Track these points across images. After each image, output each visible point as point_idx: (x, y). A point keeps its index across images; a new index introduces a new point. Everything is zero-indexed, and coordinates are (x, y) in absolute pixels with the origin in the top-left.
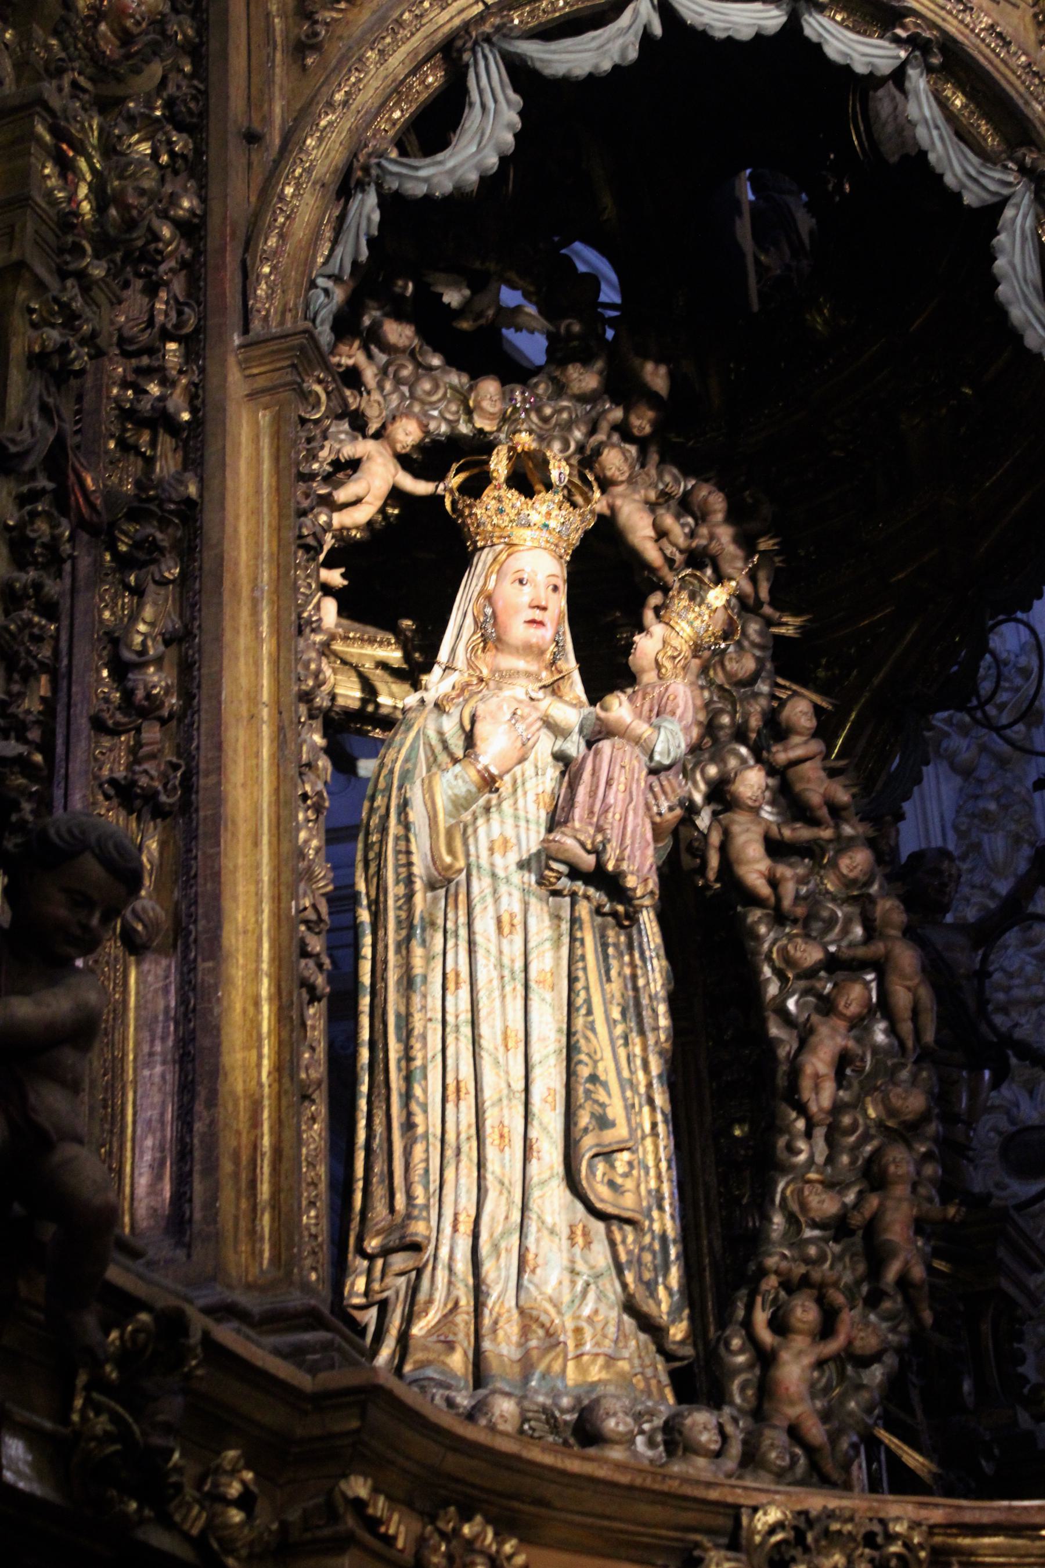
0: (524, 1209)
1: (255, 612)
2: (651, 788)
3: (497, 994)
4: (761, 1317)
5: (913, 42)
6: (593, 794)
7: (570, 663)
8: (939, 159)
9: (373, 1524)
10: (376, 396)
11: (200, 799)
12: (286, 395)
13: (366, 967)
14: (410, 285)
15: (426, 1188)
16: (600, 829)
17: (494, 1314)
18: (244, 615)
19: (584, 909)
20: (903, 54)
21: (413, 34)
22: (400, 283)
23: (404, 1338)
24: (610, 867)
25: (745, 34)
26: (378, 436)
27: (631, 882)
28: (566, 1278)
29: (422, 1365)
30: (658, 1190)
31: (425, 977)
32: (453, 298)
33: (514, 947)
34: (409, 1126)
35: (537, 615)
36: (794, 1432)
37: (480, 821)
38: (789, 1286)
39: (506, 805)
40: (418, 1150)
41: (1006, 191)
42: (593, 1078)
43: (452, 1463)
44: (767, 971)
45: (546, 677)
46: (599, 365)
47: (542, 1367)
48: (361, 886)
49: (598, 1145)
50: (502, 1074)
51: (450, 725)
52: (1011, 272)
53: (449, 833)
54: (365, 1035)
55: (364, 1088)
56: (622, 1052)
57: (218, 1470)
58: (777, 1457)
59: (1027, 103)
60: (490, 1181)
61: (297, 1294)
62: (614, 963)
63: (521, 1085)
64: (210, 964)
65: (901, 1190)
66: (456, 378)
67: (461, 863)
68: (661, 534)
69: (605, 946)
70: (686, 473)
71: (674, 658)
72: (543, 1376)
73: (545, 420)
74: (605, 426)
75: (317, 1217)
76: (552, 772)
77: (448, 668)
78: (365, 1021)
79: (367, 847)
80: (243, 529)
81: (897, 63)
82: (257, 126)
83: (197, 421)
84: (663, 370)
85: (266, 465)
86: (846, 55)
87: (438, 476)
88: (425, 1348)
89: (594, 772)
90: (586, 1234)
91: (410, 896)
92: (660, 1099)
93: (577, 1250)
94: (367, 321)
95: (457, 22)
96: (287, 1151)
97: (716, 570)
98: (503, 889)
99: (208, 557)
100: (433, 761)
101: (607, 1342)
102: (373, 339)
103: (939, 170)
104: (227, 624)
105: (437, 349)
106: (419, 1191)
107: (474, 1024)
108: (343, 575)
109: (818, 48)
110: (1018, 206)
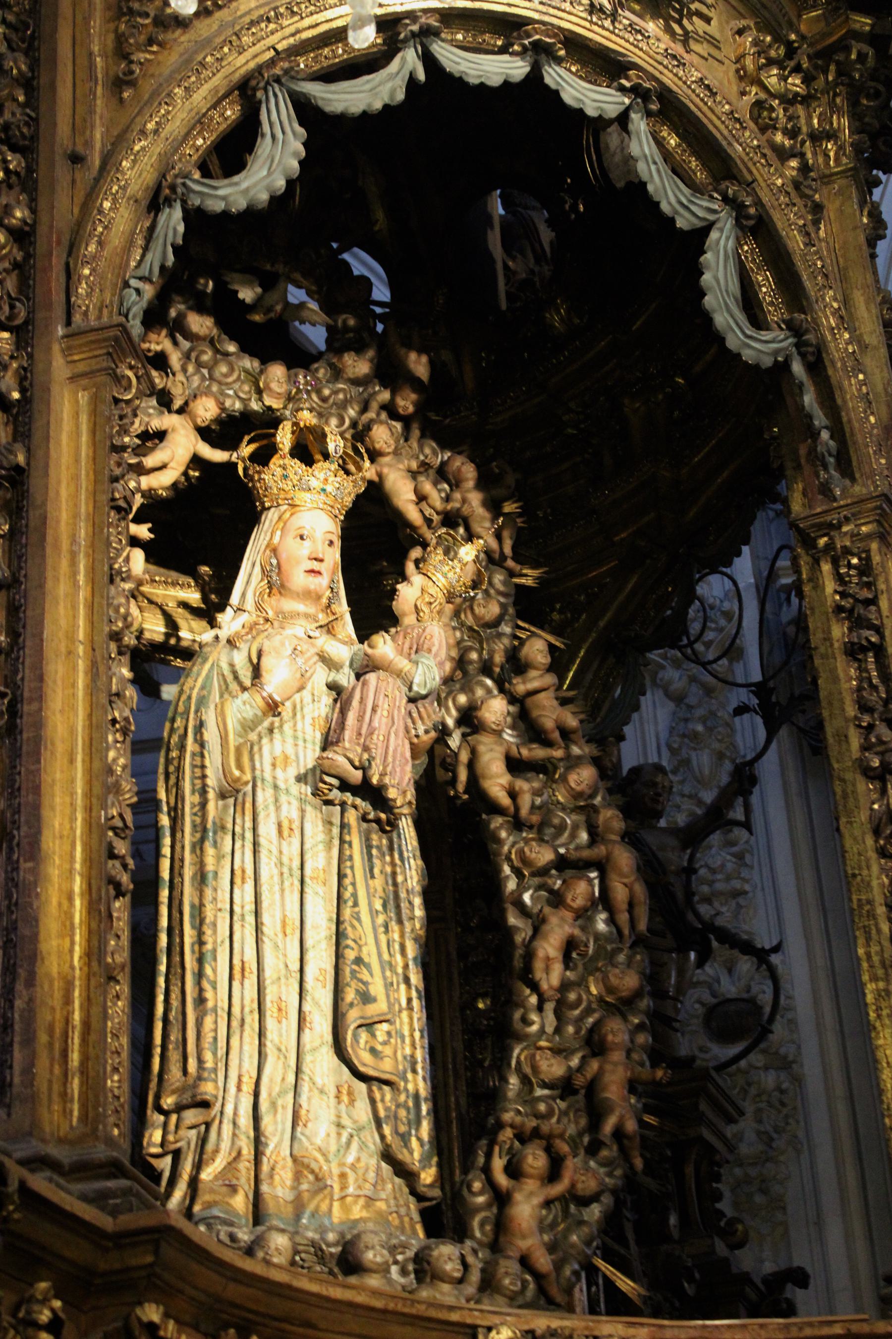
0: (298, 1071)
1: (73, 563)
2: (410, 713)
3: (277, 888)
4: (498, 1164)
5: (635, 90)
6: (360, 718)
7: (343, 608)
8: (656, 190)
10: (180, 377)
11: (24, 722)
12: (102, 378)
13: (165, 865)
14: (211, 283)
15: (215, 1054)
16: (366, 749)
17: (272, 1161)
18: (64, 564)
19: (352, 816)
20: (627, 101)
21: (214, 74)
22: (202, 281)
23: (194, 1183)
24: (375, 781)
25: (495, 81)
26: (181, 411)
27: (392, 793)
28: (333, 1130)
29: (209, 1205)
30: (412, 1056)
31: (216, 873)
32: (247, 294)
33: (292, 848)
34: (201, 1000)
35: (315, 565)
36: (525, 1262)
37: (265, 741)
38: (522, 1137)
39: (287, 727)
40: (208, 1021)
41: (711, 217)
42: (358, 961)
43: (234, 1291)
44: (507, 870)
45: (323, 619)
46: (371, 353)
47: (311, 1207)
48: (162, 795)
49: (362, 1018)
50: (281, 956)
51: (240, 659)
52: (715, 284)
53: (238, 750)
54: (164, 922)
55: (163, 968)
56: (383, 938)
57: (31, 1299)
58: (511, 1284)
59: (730, 144)
60: (270, 1049)
61: (101, 1147)
62: (377, 862)
63: (296, 966)
64: (30, 865)
65: (617, 1056)
66: (249, 363)
67: (248, 777)
68: (421, 498)
69: (369, 847)
70: (443, 446)
71: (431, 603)
72: (313, 1215)
73: (324, 400)
74: (374, 406)
75: (119, 1081)
76: (327, 699)
77: (239, 610)
78: (164, 910)
79: (168, 762)
80: (64, 493)
81: (622, 108)
82: (80, 149)
83: (26, 400)
84: (424, 359)
85: (84, 438)
86: (580, 100)
87: (231, 445)
88: (212, 1191)
89: (362, 700)
90: (350, 1093)
91: (203, 805)
92: (416, 978)
93: (343, 1107)
94: (173, 313)
95: (252, 65)
96: (95, 1025)
97: (467, 528)
98: (283, 798)
99: (33, 516)
100: (225, 690)
101: (368, 1186)
102: (177, 329)
103: (656, 199)
104: (49, 574)
105: (232, 338)
106: (208, 1056)
107: (257, 913)
108: (150, 530)
109: (556, 93)
110: (721, 230)
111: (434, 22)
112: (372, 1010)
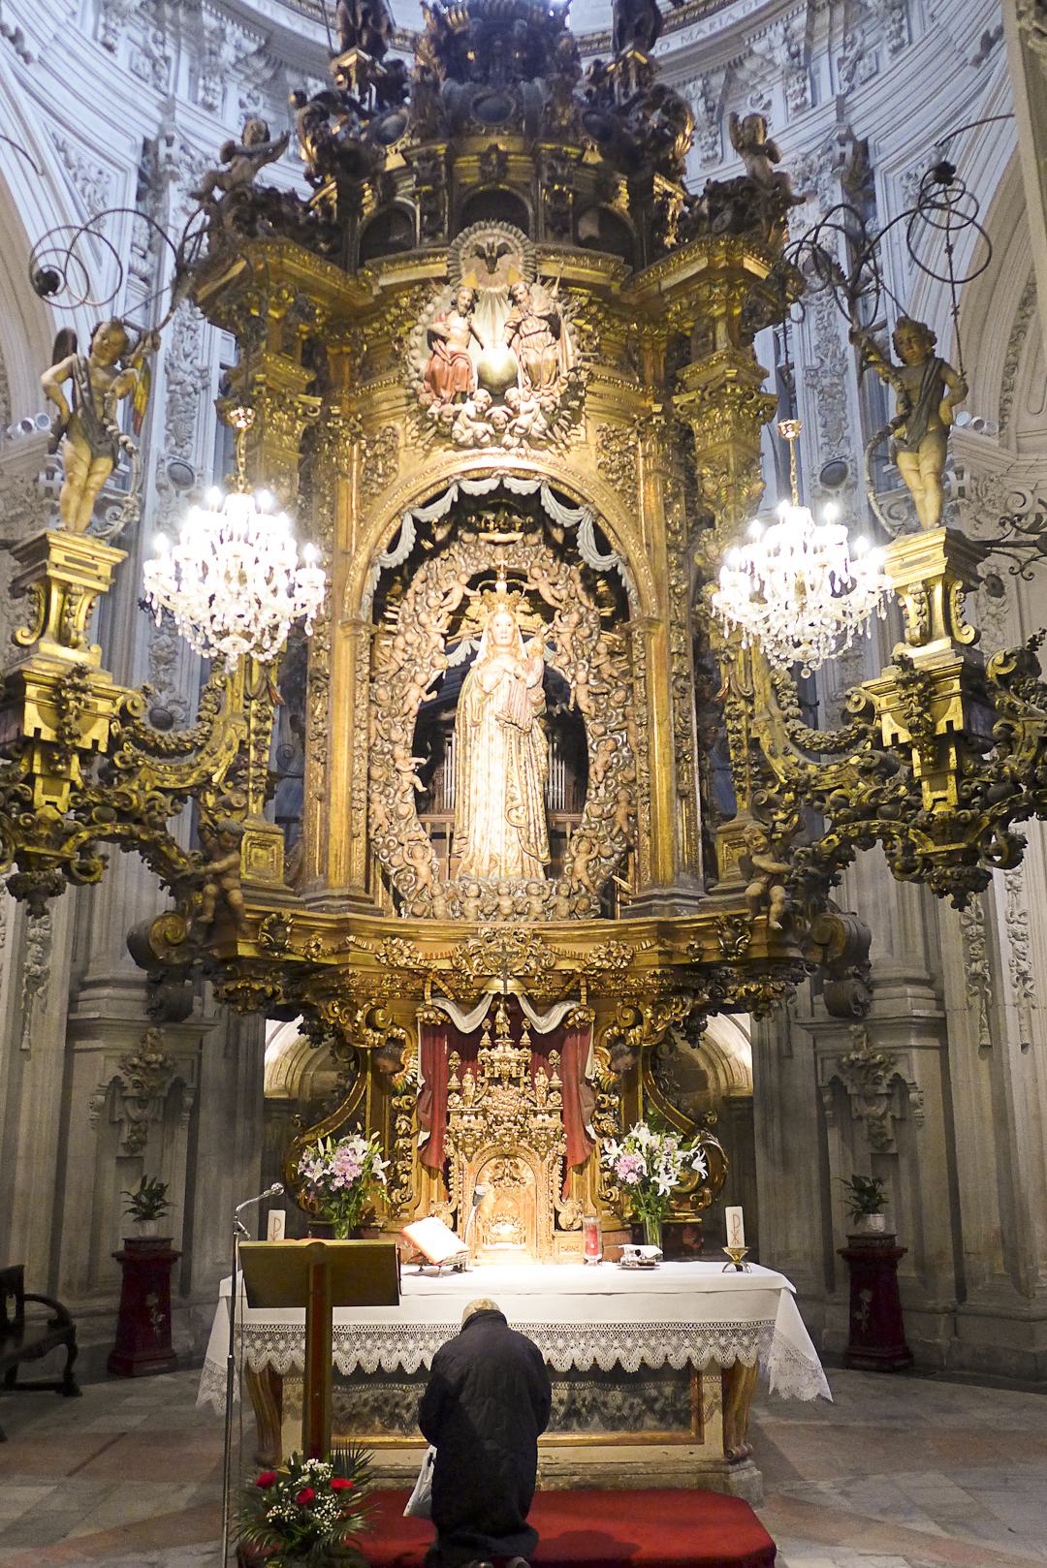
4: (573, 848)
25: (485, 492)
112: (515, 803)
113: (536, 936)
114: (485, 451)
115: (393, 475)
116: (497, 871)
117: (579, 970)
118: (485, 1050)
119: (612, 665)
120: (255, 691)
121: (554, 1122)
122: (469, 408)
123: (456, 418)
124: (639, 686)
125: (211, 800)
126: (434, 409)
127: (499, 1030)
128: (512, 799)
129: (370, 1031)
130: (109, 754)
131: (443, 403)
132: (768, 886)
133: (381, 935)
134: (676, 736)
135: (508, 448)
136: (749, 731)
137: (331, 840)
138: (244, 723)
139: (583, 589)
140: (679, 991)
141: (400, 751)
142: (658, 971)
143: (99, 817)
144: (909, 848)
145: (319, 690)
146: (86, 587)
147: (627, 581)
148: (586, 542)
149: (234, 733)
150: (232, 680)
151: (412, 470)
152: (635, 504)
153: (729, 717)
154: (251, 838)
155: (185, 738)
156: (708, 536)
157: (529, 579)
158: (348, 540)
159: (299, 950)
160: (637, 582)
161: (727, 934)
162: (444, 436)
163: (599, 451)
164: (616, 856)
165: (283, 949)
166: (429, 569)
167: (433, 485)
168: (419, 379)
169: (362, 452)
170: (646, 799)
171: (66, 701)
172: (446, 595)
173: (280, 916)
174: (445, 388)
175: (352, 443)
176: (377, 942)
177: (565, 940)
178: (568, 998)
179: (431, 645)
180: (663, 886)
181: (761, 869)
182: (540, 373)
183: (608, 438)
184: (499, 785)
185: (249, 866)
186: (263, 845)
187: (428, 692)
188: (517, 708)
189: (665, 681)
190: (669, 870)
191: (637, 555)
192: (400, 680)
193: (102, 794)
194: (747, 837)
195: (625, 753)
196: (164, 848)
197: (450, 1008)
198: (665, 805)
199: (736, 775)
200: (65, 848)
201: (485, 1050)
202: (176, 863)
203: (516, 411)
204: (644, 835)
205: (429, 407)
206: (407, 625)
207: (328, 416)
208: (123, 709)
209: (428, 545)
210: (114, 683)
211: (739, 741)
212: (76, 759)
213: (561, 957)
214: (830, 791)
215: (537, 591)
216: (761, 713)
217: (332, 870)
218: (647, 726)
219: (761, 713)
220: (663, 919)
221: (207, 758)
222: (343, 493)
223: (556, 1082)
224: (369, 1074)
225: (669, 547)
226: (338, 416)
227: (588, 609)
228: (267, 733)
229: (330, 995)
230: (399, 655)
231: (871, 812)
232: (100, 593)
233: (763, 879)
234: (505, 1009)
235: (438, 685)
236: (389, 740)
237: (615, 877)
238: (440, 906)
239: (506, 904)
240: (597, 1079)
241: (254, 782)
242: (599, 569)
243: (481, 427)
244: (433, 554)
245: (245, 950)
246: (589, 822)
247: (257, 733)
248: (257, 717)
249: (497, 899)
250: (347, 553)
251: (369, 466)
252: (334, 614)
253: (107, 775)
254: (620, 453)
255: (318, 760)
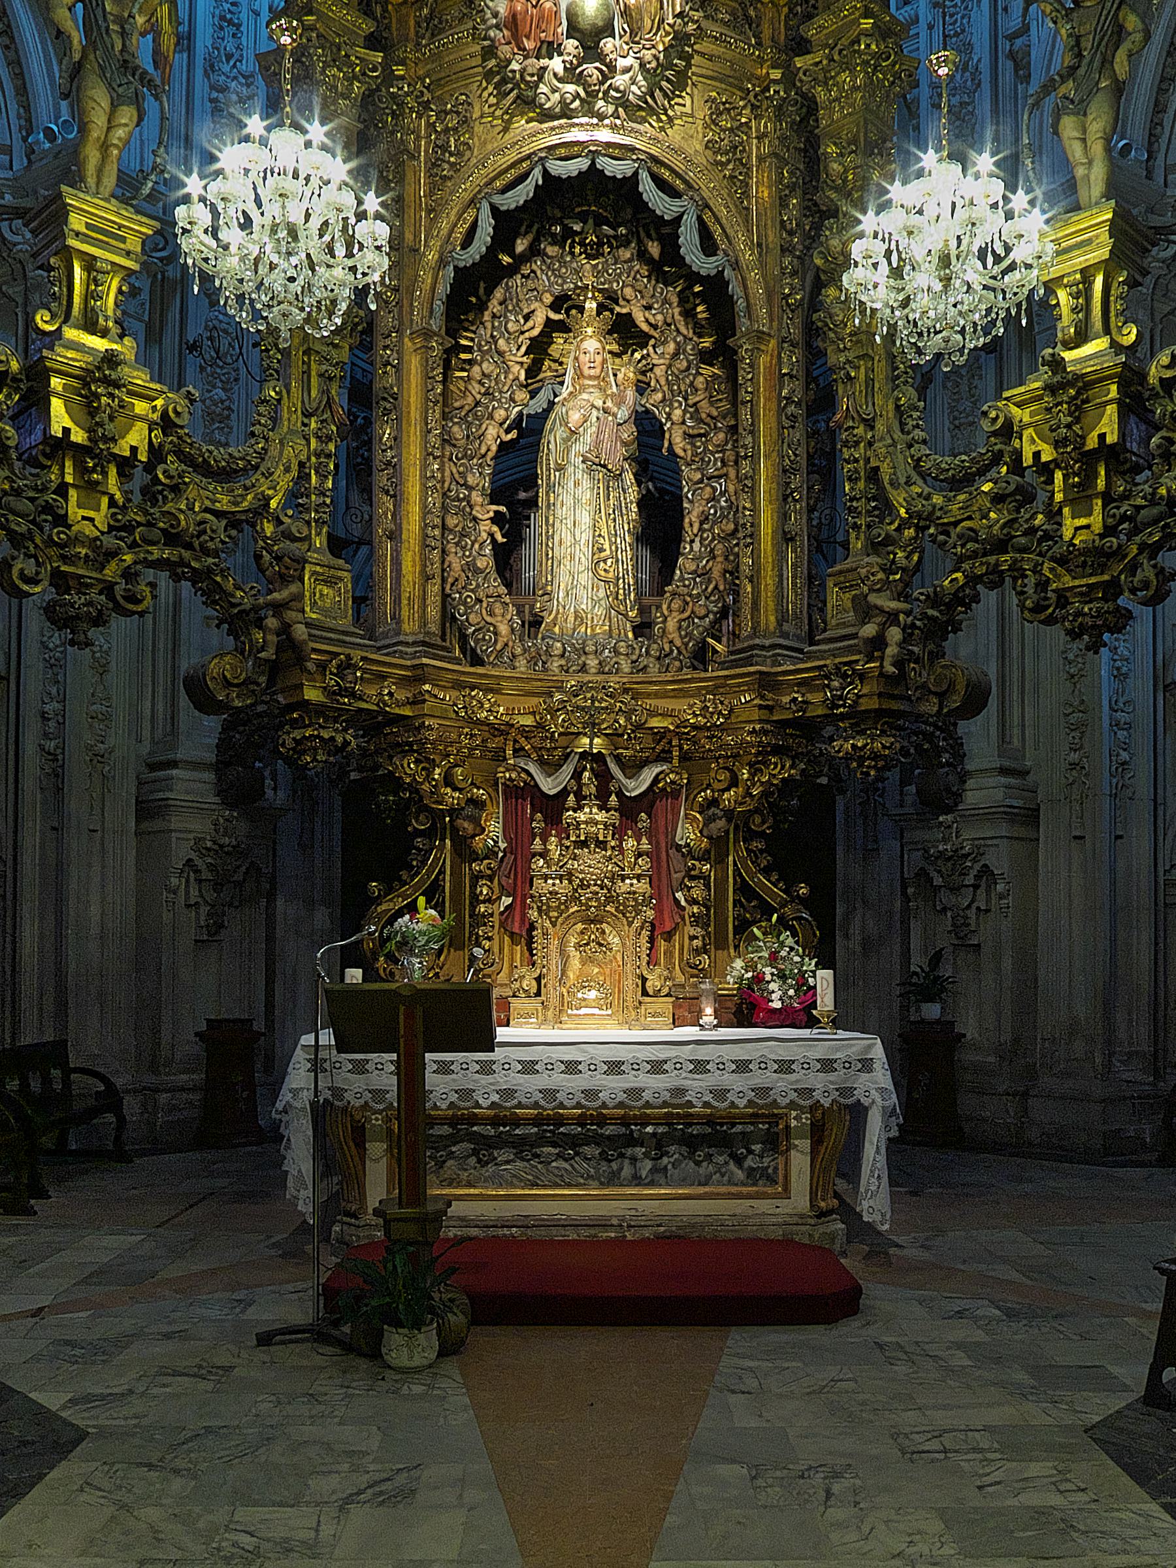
9: (436, 696)
36: (671, 642)
41: (682, 210)
65: (719, 559)
84: (655, 244)
111: (543, 155)
113: (626, 691)
114: (576, 121)
115: (468, 153)
116: (583, 630)
117: (672, 728)
118: (571, 813)
119: (711, 404)
120: (314, 405)
121: (642, 887)
122: (556, 64)
123: (541, 78)
124: (745, 414)
125: (269, 529)
126: (515, 66)
127: (586, 791)
128: (601, 550)
129: (449, 790)
130: (149, 467)
131: (526, 57)
132: (883, 627)
133: (458, 685)
134: (785, 471)
135: (601, 117)
136: (868, 460)
137: (404, 582)
138: (304, 442)
139: (680, 314)
140: (777, 750)
141: (476, 497)
142: (758, 727)
143: (144, 540)
144: (1042, 585)
145: (386, 412)
146: (113, 263)
147: (734, 288)
148: (688, 238)
149: (295, 451)
150: (288, 392)
151: (489, 147)
152: (746, 194)
153: (846, 444)
154: (314, 573)
155: (236, 454)
156: (831, 229)
157: (621, 302)
158: (416, 235)
159: (372, 696)
160: (745, 287)
161: (836, 684)
162: (527, 103)
163: (706, 126)
164: (711, 616)
165: (353, 695)
166: (508, 288)
167: (513, 165)
168: (497, 26)
169: (431, 126)
170: (749, 540)
171: (97, 396)
172: (527, 318)
173: (349, 657)
174: (528, 38)
175: (419, 117)
176: (455, 693)
177: (656, 695)
178: (658, 759)
179: (511, 377)
180: (764, 637)
181: (876, 607)
182: (642, 19)
183: (718, 111)
184: (585, 536)
185: (314, 604)
186: (330, 582)
187: (507, 432)
188: (606, 445)
189: (774, 406)
190: (772, 618)
191: (748, 256)
192: (476, 417)
193: (146, 513)
194: (863, 572)
195: (723, 504)
196: (218, 579)
197: (532, 768)
198: (769, 548)
199: (851, 510)
200: (106, 571)
201: (571, 813)
202: (233, 596)
203: (612, 67)
204: (746, 581)
205: (509, 62)
206: (484, 353)
207: (389, 78)
208: (165, 414)
209: (506, 259)
210: (152, 380)
211: (856, 471)
212: (113, 471)
213: (653, 713)
214: (956, 524)
215: (629, 315)
216: (882, 439)
217: (405, 613)
218: (754, 459)
219: (882, 439)
220: (763, 669)
221: (263, 480)
222: (410, 176)
223: (645, 846)
224: (448, 842)
225: (783, 250)
226: (402, 78)
227: (685, 336)
228: (329, 456)
229: (404, 749)
230: (475, 388)
231: (1001, 545)
232: (130, 273)
233: (879, 619)
234: (592, 769)
235: (517, 423)
236: (465, 485)
237: (710, 640)
238: (521, 664)
239: (592, 662)
240: (688, 845)
241: (317, 511)
242: (703, 272)
243: (571, 88)
244: (512, 270)
245: (312, 694)
246: (682, 579)
247: (318, 456)
248: (318, 438)
249: (583, 659)
250: (417, 250)
251: (439, 143)
252: (401, 323)
253: (150, 494)
254: (731, 130)
255: (387, 493)
